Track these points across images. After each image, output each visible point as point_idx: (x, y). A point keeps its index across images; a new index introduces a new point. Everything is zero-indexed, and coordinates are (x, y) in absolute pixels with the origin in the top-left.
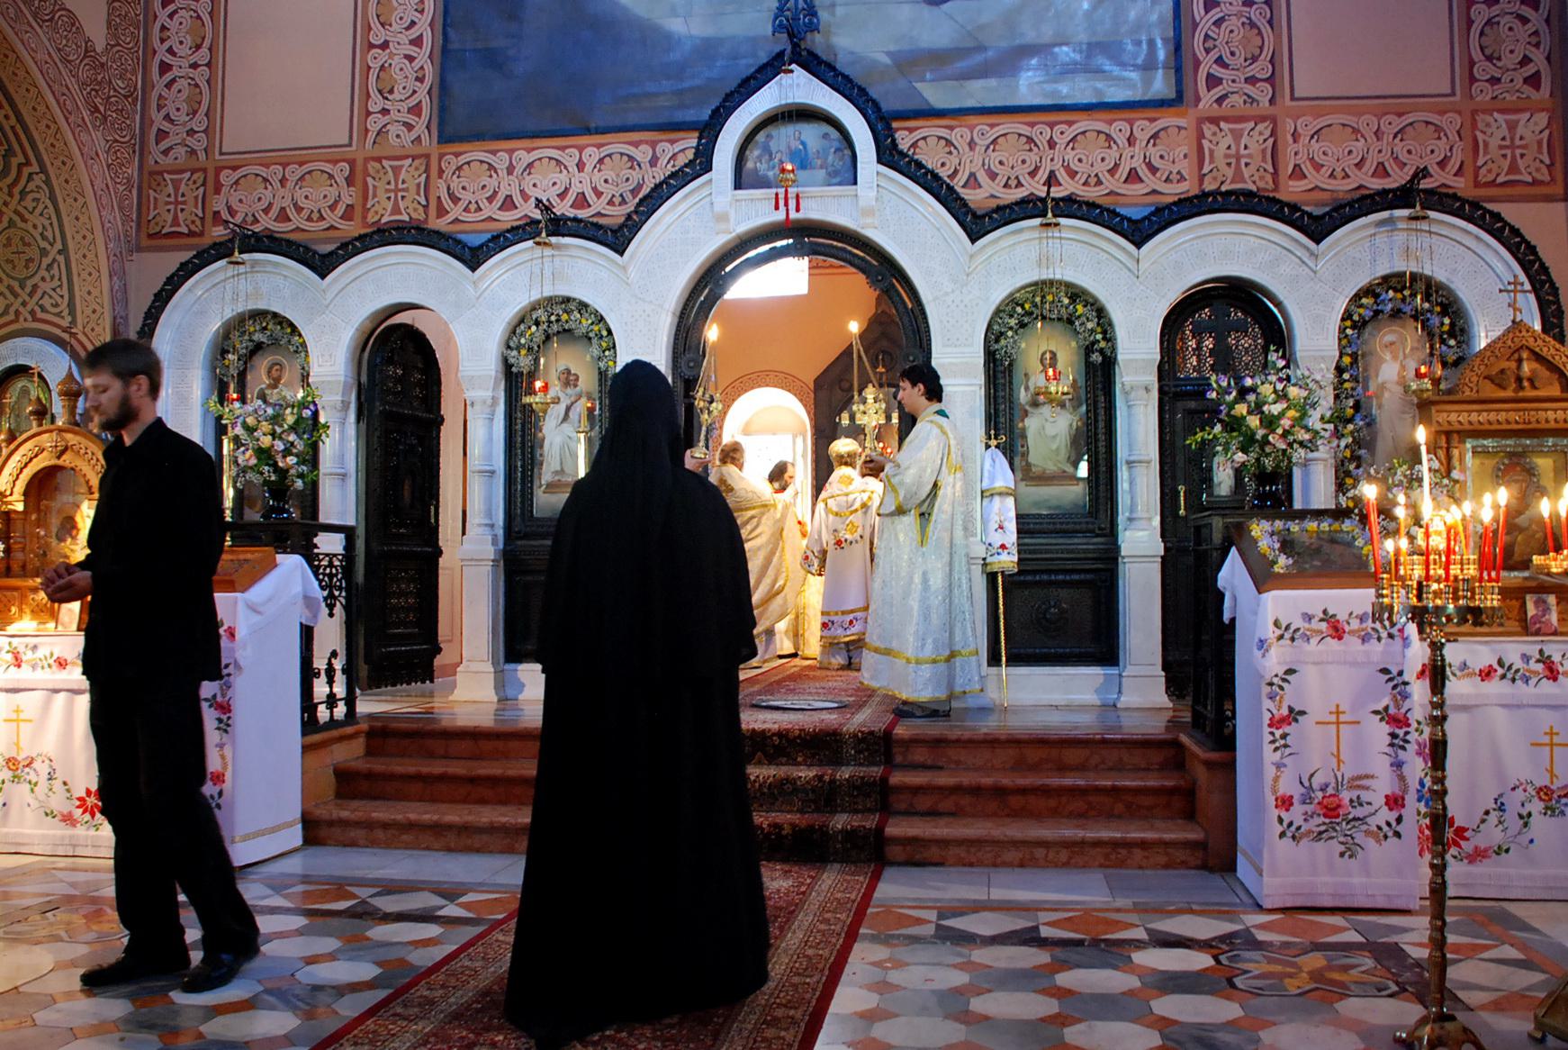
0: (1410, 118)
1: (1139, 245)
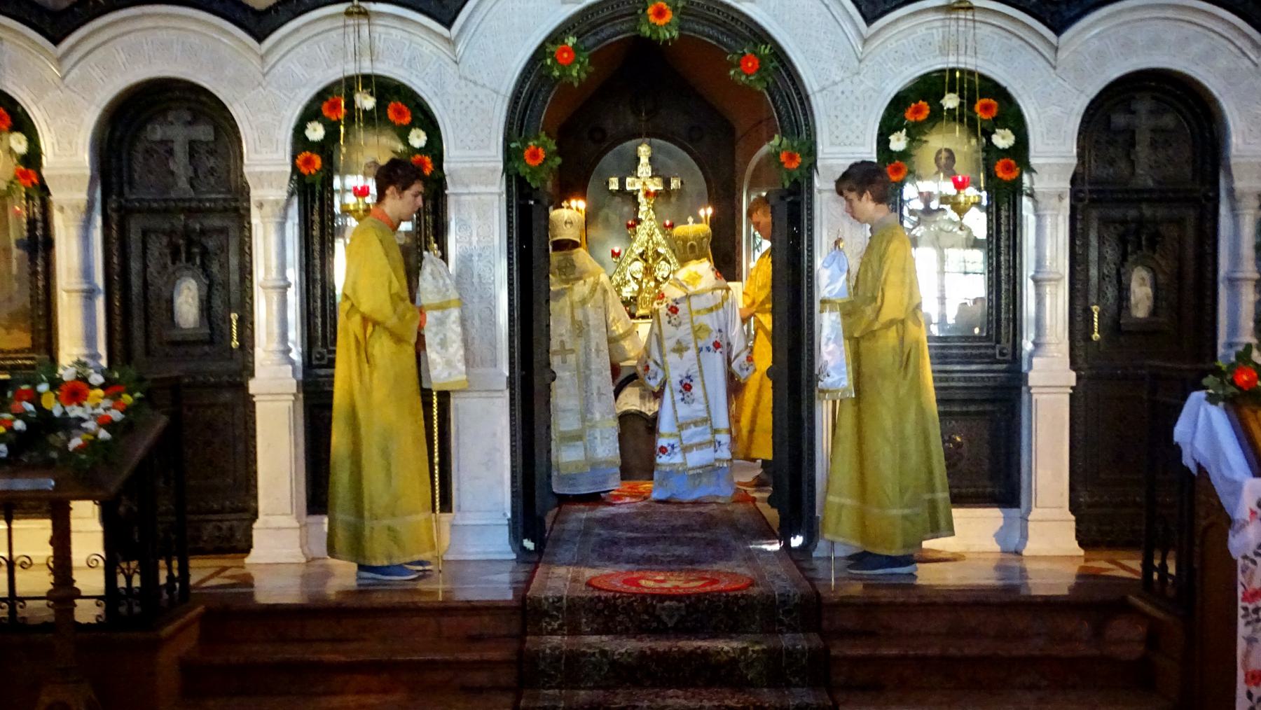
1: (1058, 31)
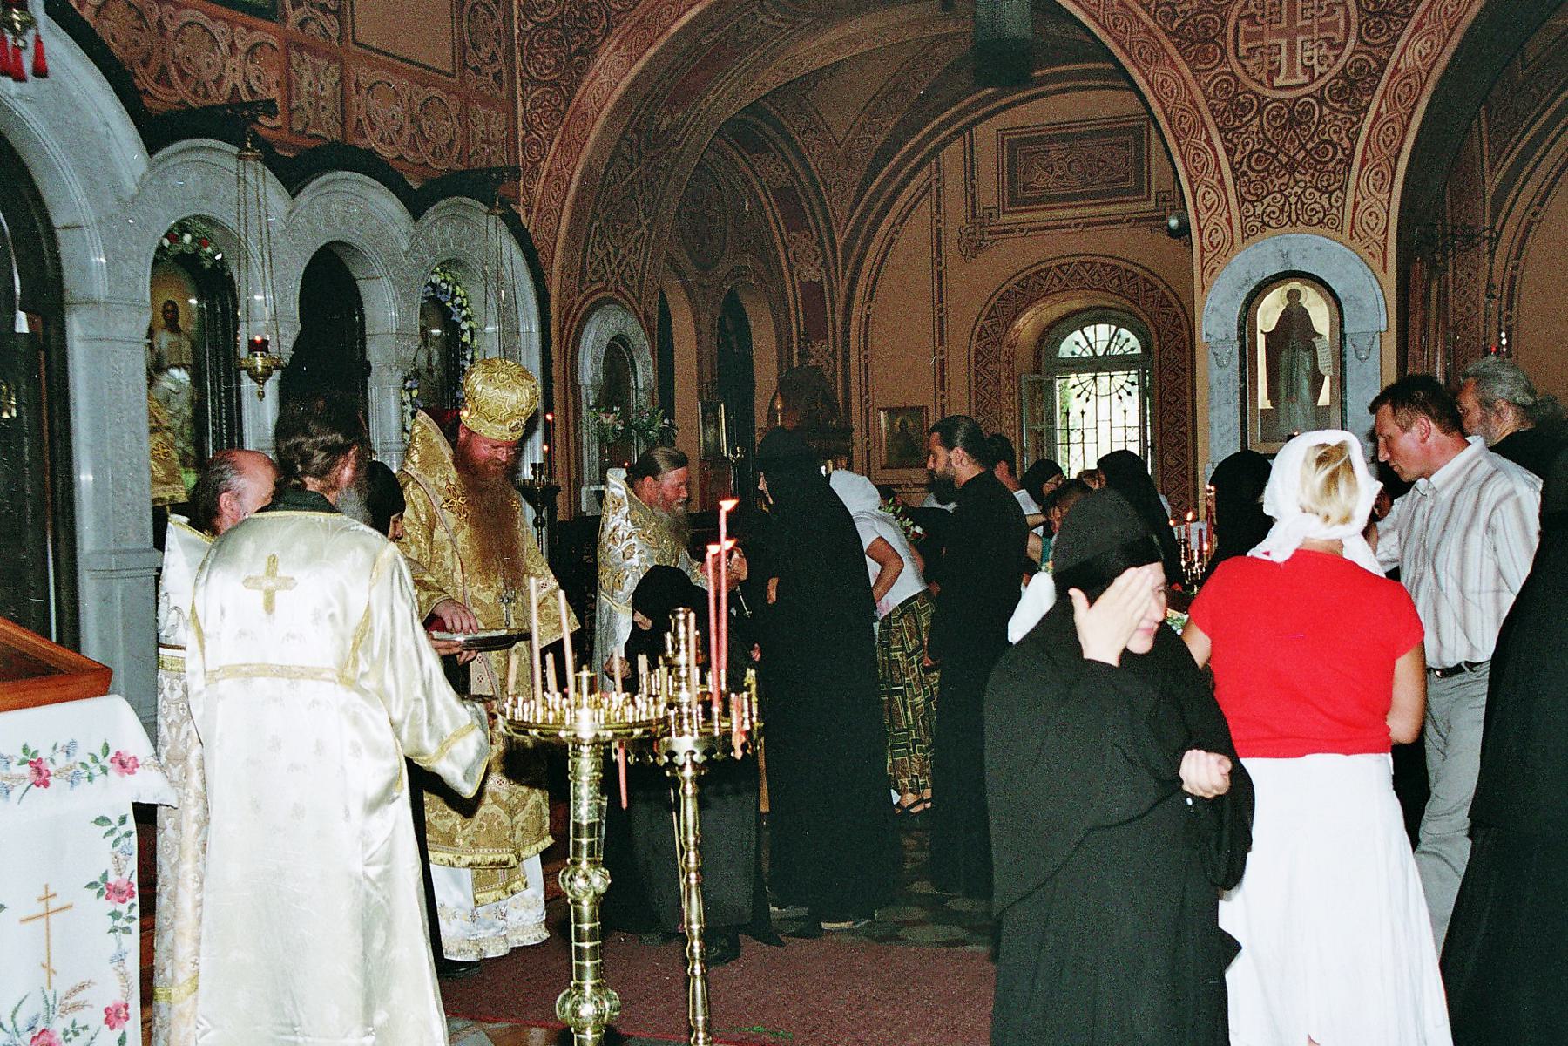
0: (434, 92)
